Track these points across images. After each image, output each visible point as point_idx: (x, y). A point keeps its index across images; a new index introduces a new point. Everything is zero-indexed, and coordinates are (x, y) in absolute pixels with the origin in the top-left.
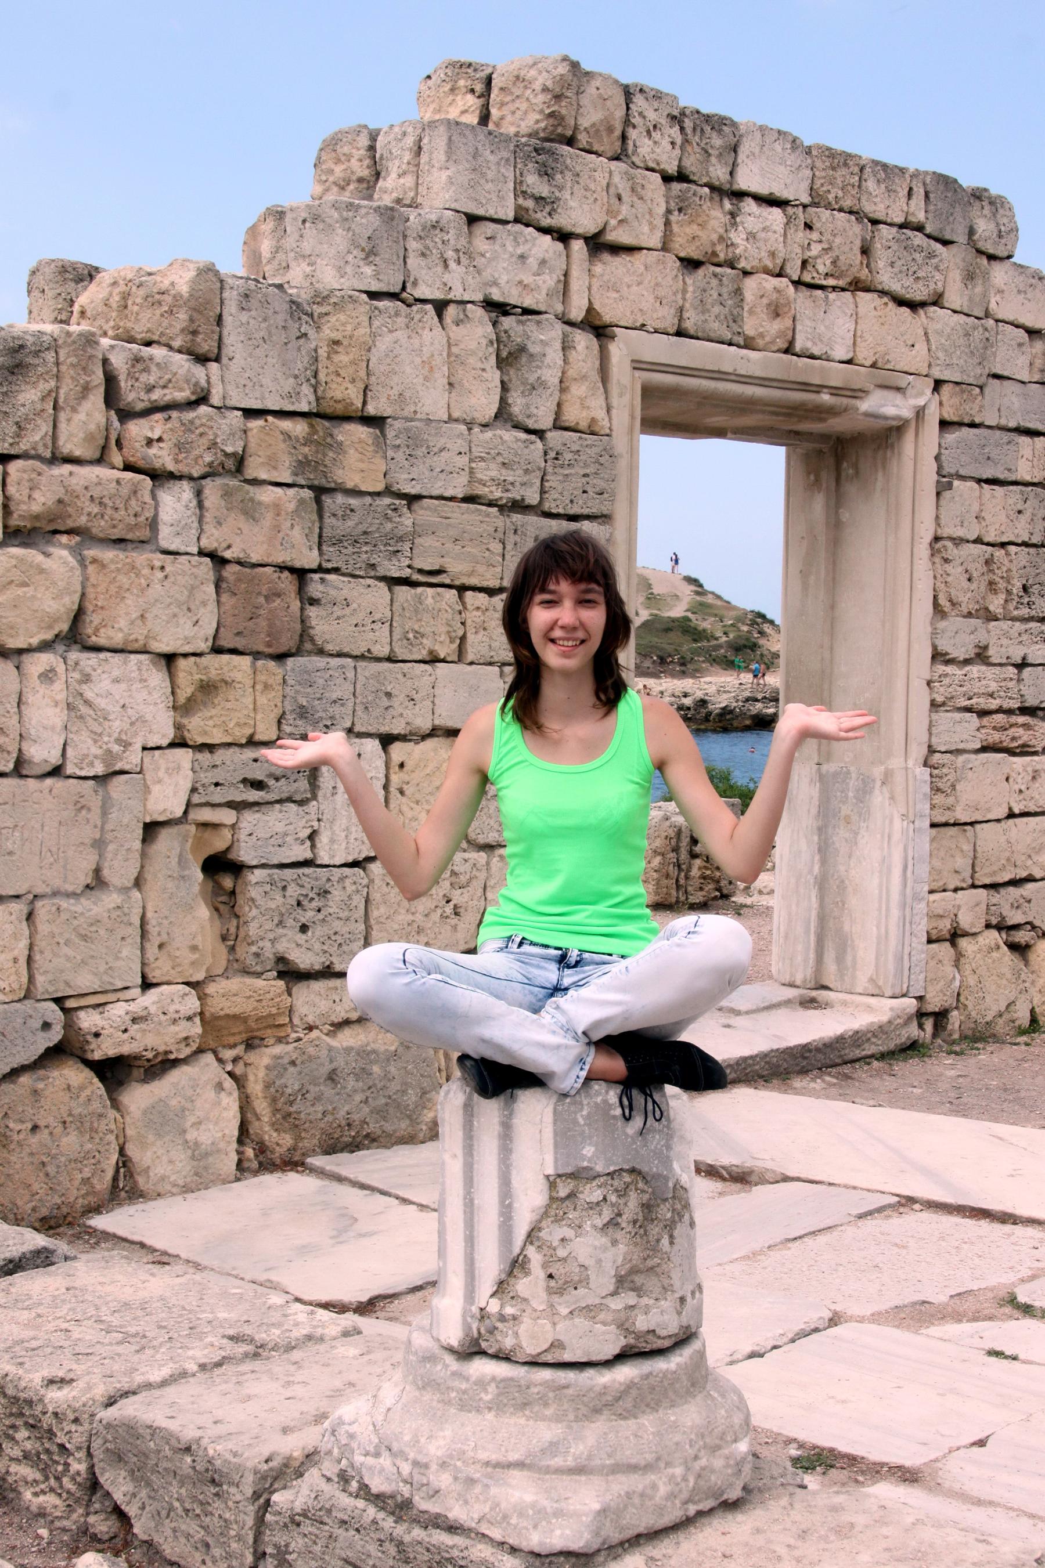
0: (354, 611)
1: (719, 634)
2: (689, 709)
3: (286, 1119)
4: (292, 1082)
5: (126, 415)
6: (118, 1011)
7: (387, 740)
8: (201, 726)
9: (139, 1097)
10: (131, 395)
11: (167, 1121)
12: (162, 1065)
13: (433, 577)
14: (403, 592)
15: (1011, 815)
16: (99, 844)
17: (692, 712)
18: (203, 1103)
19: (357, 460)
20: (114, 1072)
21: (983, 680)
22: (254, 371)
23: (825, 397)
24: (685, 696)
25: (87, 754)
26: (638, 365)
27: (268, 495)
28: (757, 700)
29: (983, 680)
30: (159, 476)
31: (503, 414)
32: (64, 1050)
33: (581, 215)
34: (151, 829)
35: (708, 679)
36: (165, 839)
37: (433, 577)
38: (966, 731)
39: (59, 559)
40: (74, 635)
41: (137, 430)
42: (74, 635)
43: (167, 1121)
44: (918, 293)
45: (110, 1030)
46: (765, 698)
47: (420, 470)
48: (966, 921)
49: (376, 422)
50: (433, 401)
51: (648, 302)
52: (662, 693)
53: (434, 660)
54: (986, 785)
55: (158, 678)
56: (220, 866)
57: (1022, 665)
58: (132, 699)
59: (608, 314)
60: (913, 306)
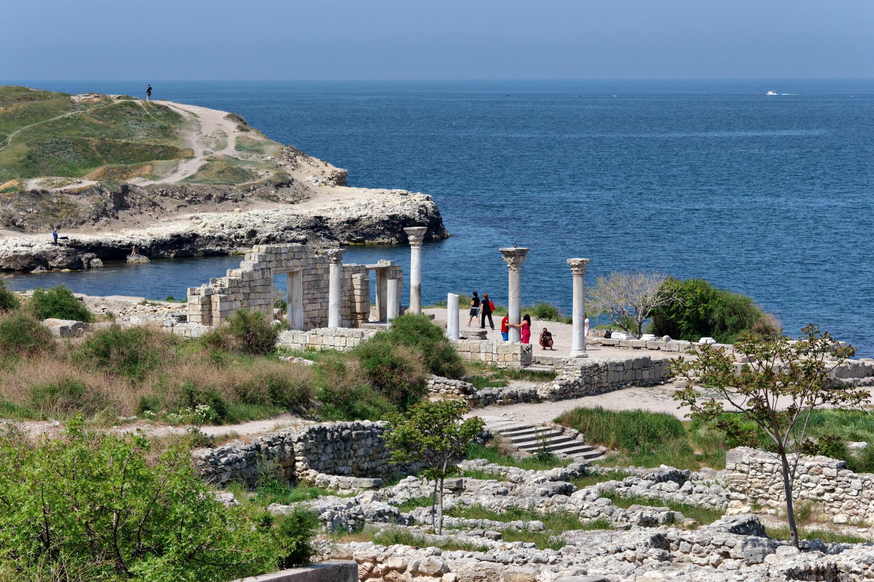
0: (252, 296)
1: (260, 173)
2: (243, 237)
17: (246, 239)
19: (252, 284)
21: (309, 296)
22: (246, 279)
24: (240, 227)
28: (292, 229)
29: (309, 296)
33: (268, 259)
35: (256, 211)
38: (307, 301)
46: (298, 227)
52: (223, 225)
54: (309, 307)
58: (238, 304)
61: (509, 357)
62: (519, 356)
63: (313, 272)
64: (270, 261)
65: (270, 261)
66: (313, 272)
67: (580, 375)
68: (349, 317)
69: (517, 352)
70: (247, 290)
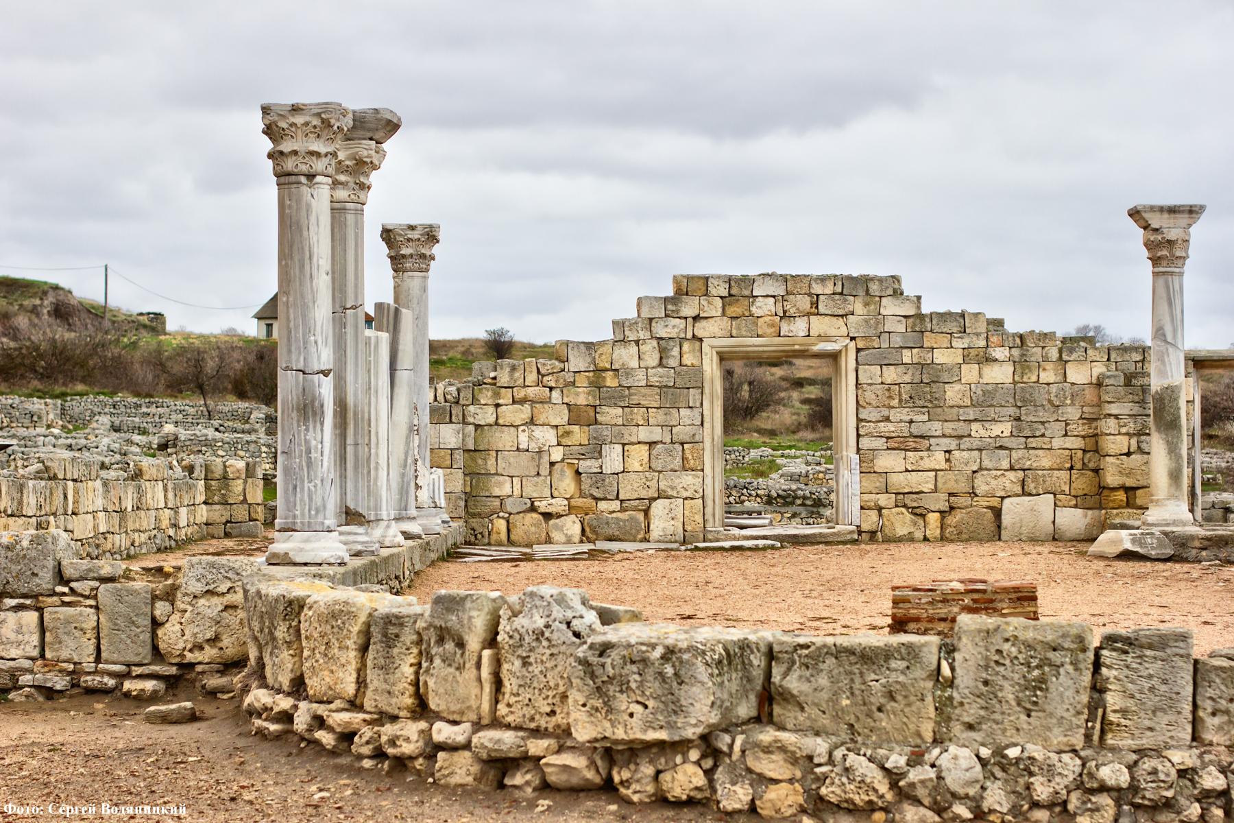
3: (594, 531)
4: (595, 523)
5: (543, 376)
6: (544, 503)
7: (624, 445)
8: (565, 441)
9: (552, 522)
10: (543, 371)
11: (560, 529)
12: (559, 516)
13: (638, 405)
14: (627, 410)
15: (907, 471)
16: (538, 466)
18: (572, 526)
20: (547, 516)
23: (797, 347)
25: (533, 447)
26: (712, 347)
27: (580, 390)
30: (551, 389)
31: (661, 365)
32: (533, 509)
34: (552, 464)
36: (557, 466)
37: (638, 405)
39: (527, 406)
40: (532, 422)
41: (546, 379)
42: (532, 422)
43: (560, 529)
44: (841, 312)
45: (542, 506)
47: (631, 380)
48: (882, 503)
49: (617, 370)
50: (634, 363)
51: (716, 330)
53: (638, 426)
55: (553, 432)
56: (578, 473)
57: (911, 422)
58: (546, 436)
59: (699, 333)
60: (842, 316)
64: (696, 318)
65: (696, 318)
66: (907, 356)
68: (1090, 501)
70: (582, 397)
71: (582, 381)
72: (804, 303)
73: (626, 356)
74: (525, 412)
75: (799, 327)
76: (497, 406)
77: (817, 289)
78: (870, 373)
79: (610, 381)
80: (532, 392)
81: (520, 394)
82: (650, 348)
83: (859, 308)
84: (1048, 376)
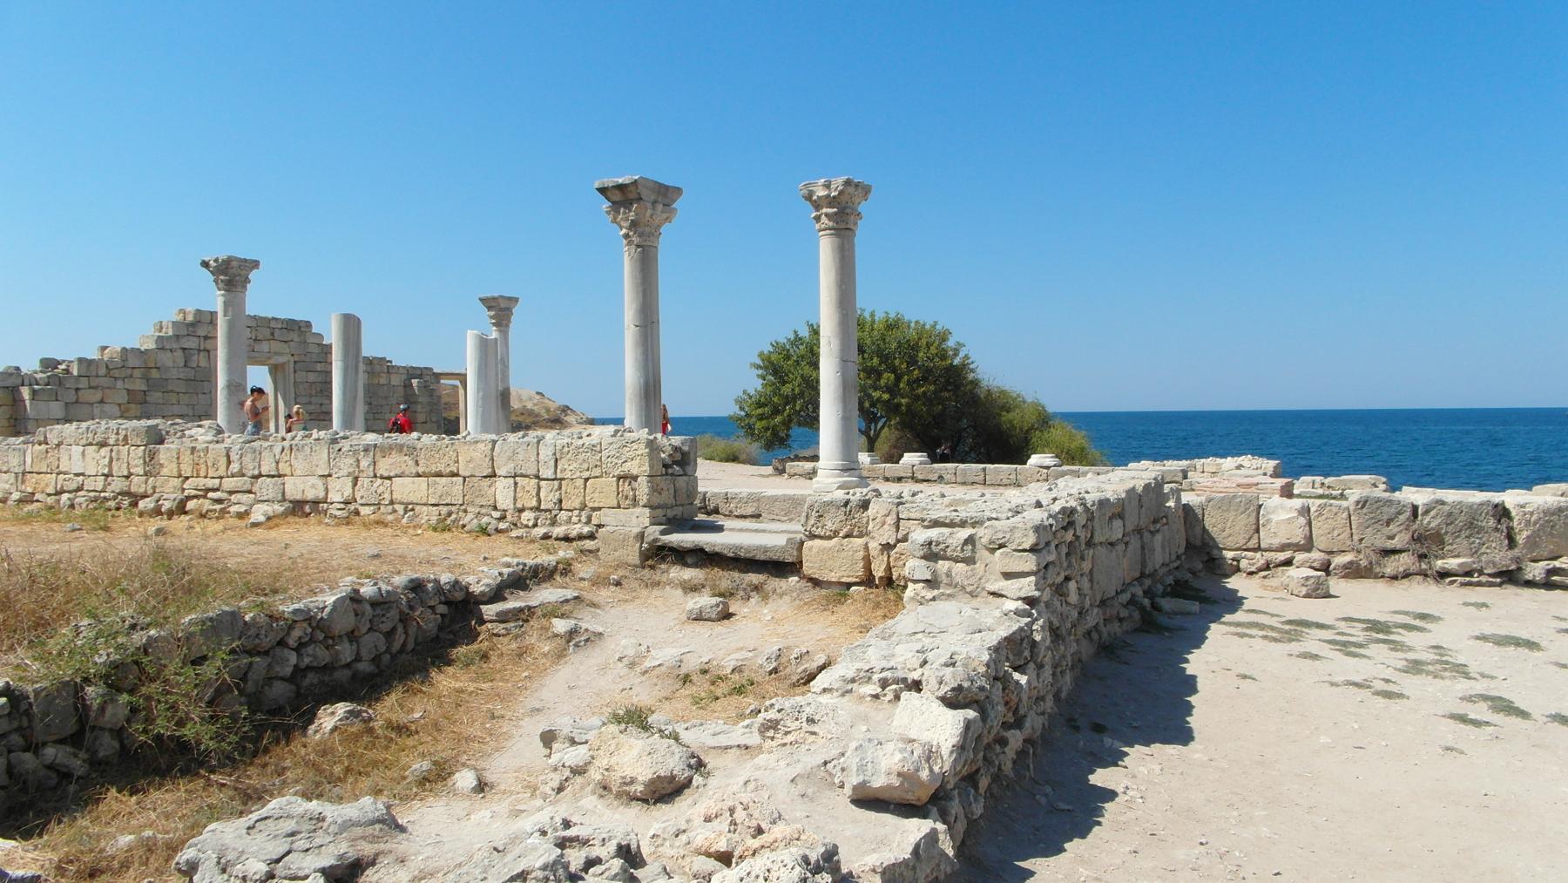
0: (155, 396)
40: (102, 402)
42: (102, 402)
50: (170, 364)
61: (603, 491)
62: (643, 488)
63: (319, 367)
67: (1027, 586)
69: (633, 467)
70: (140, 385)
71: (137, 373)
72: (267, 332)
73: (166, 359)
74: (98, 396)
75: (265, 346)
76: (77, 390)
77: (273, 325)
78: (301, 376)
79: (155, 374)
80: (104, 381)
81: (94, 382)
82: (180, 353)
83: (296, 339)
84: (383, 381)
